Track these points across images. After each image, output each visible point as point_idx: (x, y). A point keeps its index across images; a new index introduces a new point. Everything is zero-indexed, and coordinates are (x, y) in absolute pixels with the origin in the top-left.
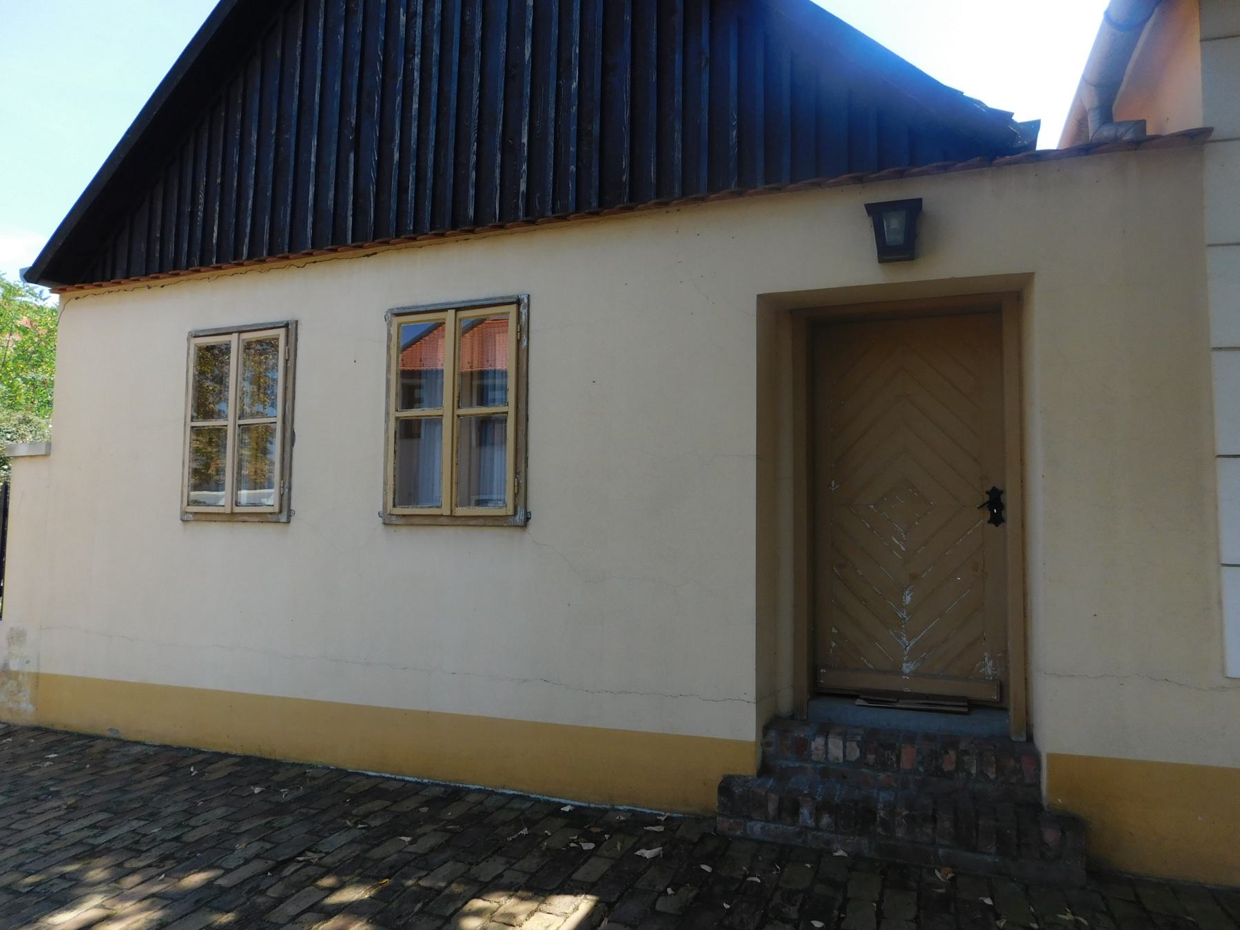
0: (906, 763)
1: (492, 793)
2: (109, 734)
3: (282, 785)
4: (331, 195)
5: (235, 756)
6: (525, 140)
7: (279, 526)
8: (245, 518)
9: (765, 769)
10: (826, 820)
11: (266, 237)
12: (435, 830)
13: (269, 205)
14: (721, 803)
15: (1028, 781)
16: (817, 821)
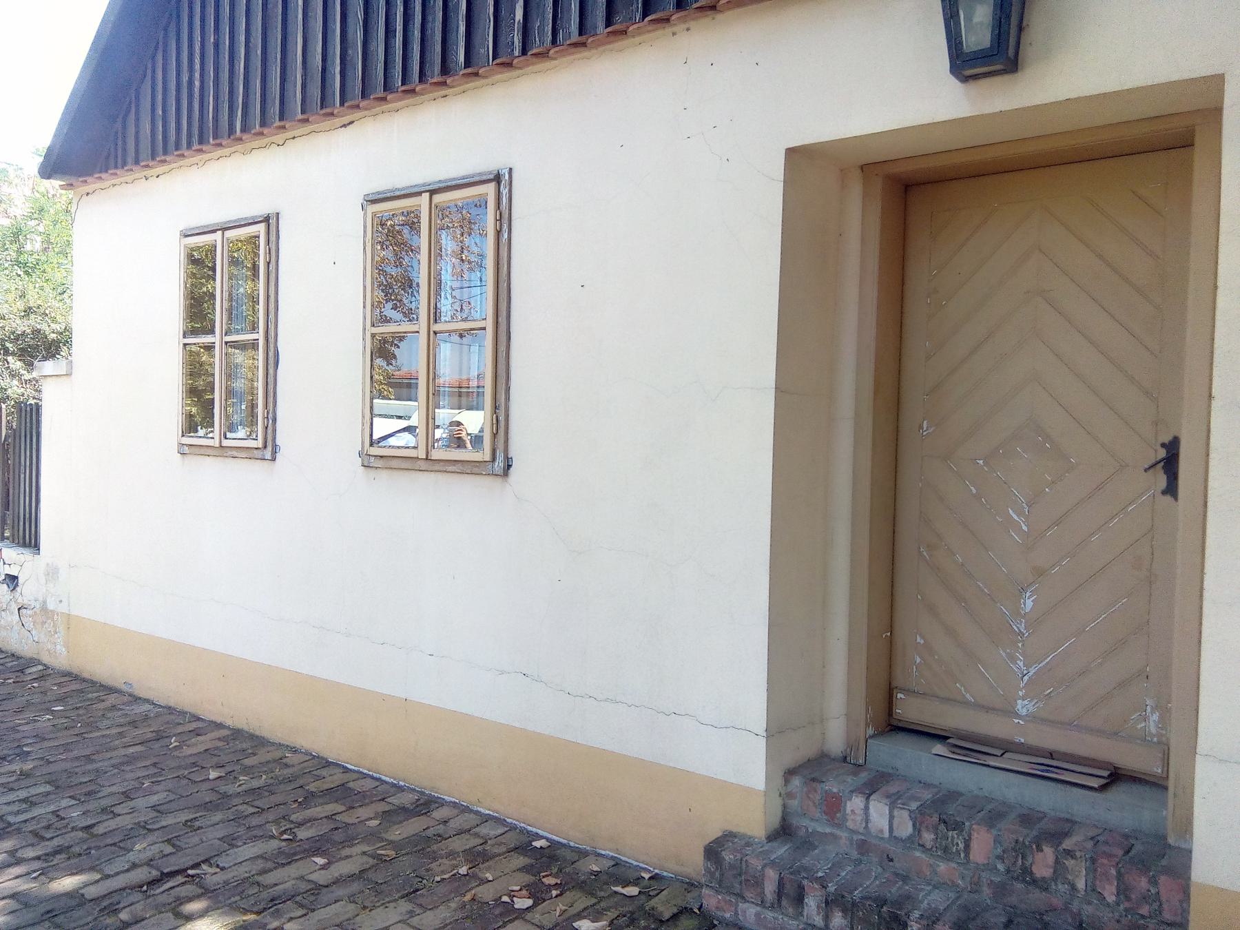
1: (467, 810)
2: (124, 688)
3: (247, 770)
5: (228, 728)
8: (235, 453)
9: (784, 831)
10: (838, 919)
12: (364, 853)
14: (707, 870)
15: (1167, 916)
16: (827, 918)
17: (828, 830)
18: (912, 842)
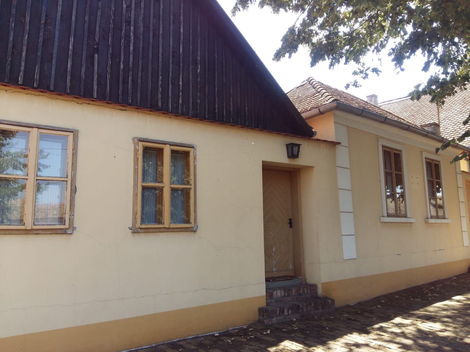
0: (293, 294)
4: (83, 70)
6: (181, 83)
7: (64, 236)
8: (40, 232)
11: (37, 76)
13: (39, 60)
17: (270, 301)
18: (284, 296)
